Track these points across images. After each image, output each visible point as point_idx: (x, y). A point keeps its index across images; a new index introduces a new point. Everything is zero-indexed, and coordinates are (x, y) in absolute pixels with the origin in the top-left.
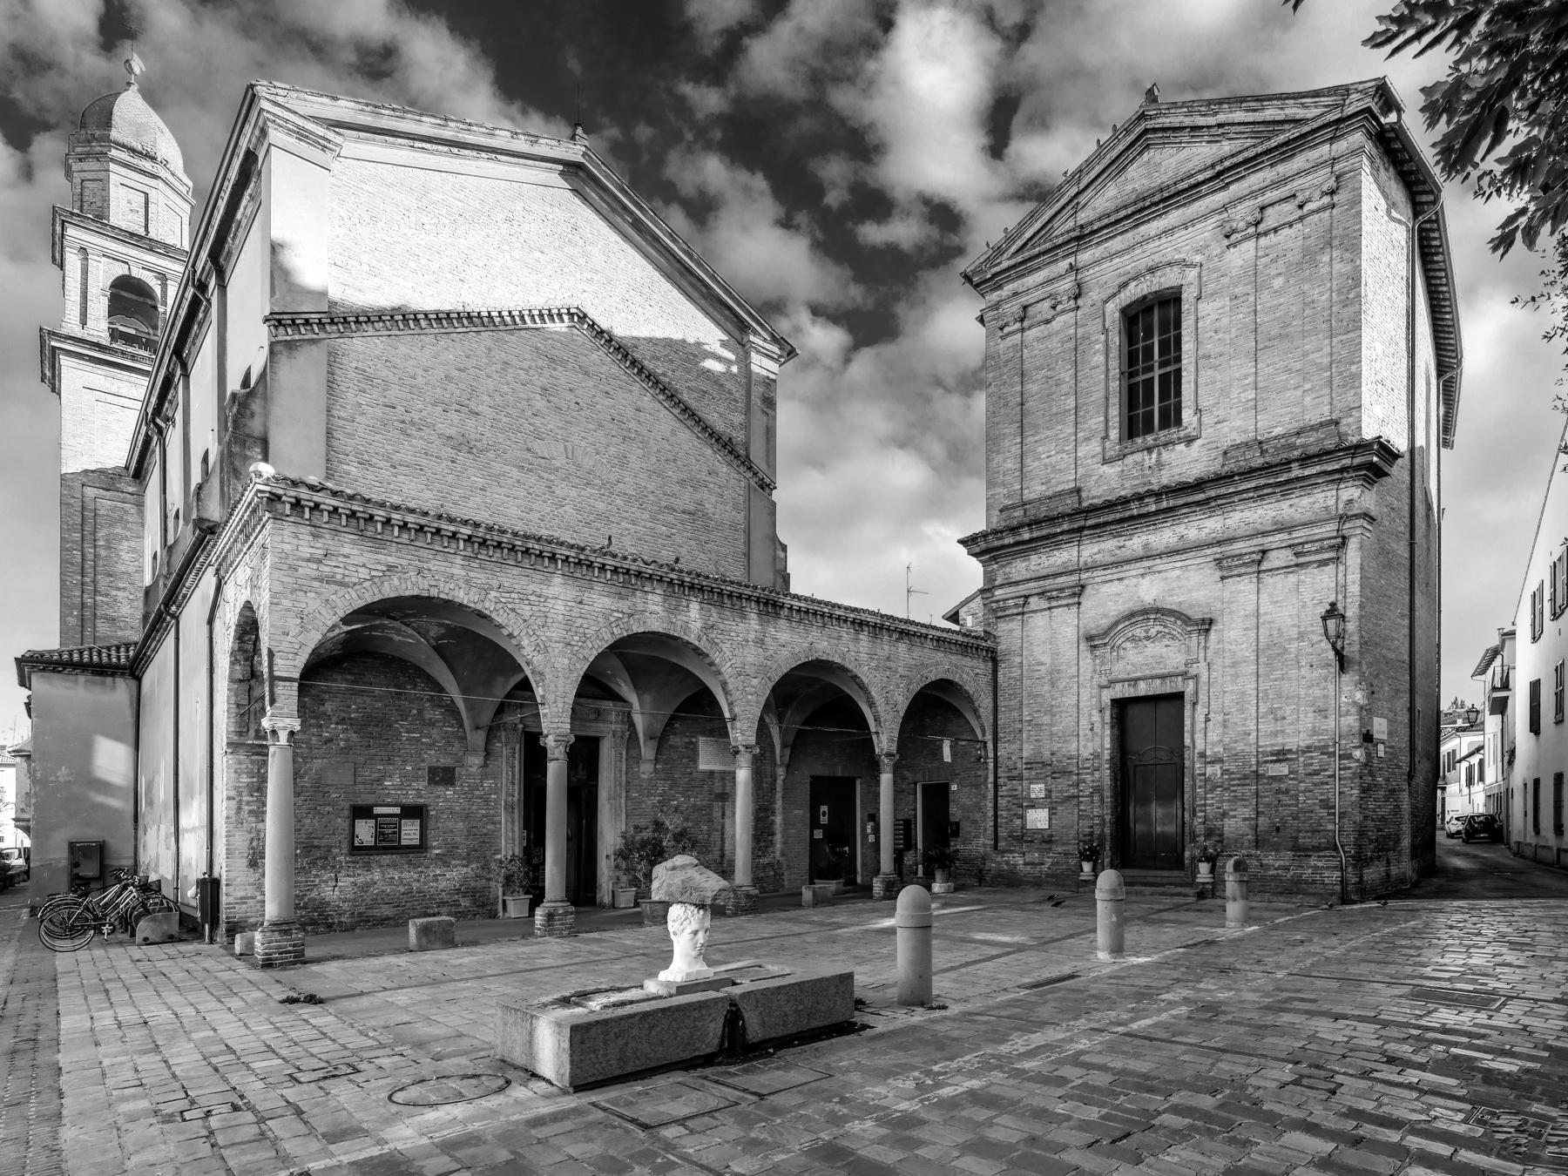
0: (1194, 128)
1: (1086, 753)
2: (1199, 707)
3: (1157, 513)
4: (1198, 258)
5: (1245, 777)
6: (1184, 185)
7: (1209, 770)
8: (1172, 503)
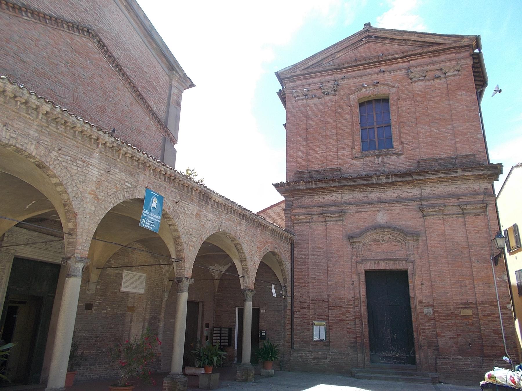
0: (391, 39)
1: (350, 297)
2: (416, 277)
3: (385, 184)
4: (396, 85)
5: (448, 315)
6: (390, 57)
7: (425, 310)
8: (394, 180)
